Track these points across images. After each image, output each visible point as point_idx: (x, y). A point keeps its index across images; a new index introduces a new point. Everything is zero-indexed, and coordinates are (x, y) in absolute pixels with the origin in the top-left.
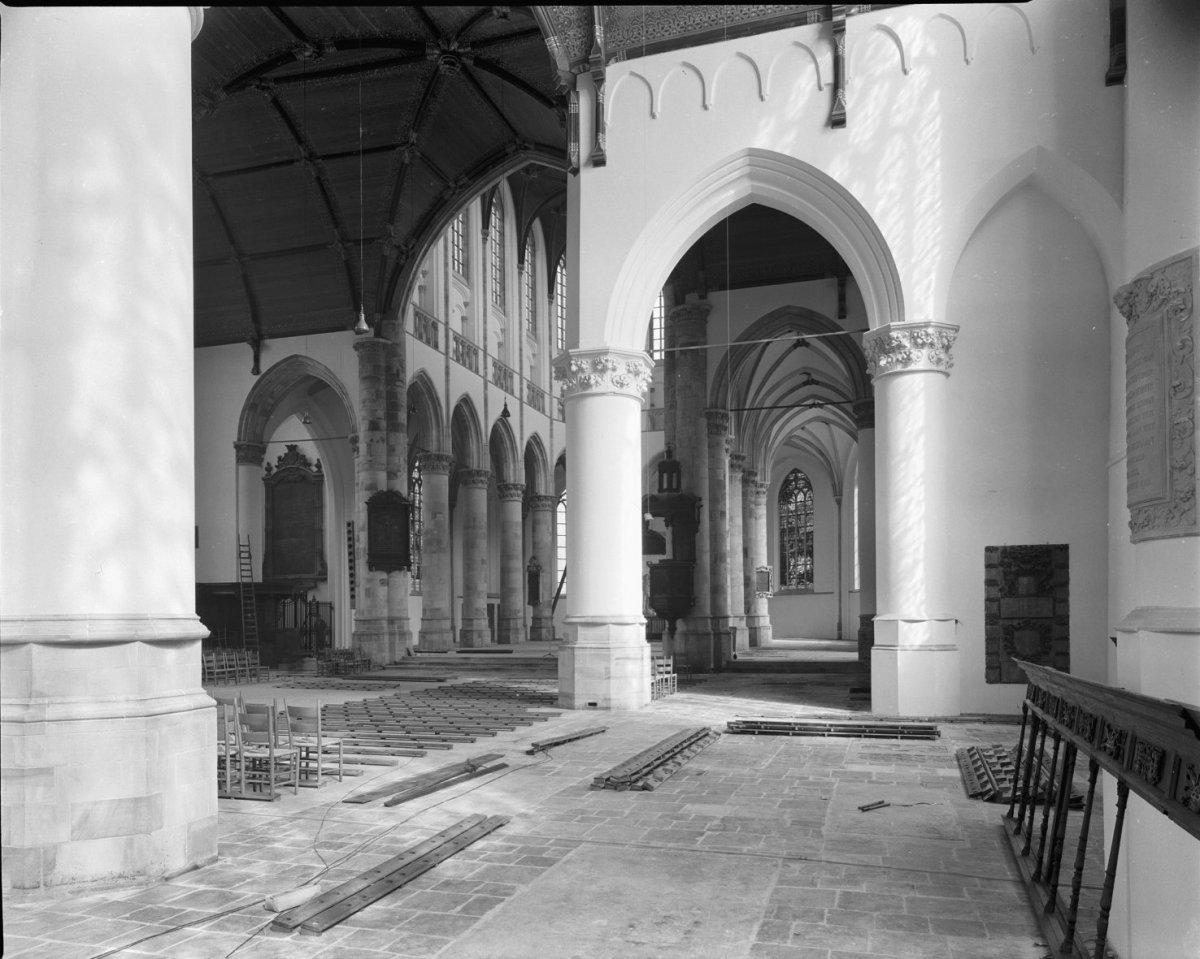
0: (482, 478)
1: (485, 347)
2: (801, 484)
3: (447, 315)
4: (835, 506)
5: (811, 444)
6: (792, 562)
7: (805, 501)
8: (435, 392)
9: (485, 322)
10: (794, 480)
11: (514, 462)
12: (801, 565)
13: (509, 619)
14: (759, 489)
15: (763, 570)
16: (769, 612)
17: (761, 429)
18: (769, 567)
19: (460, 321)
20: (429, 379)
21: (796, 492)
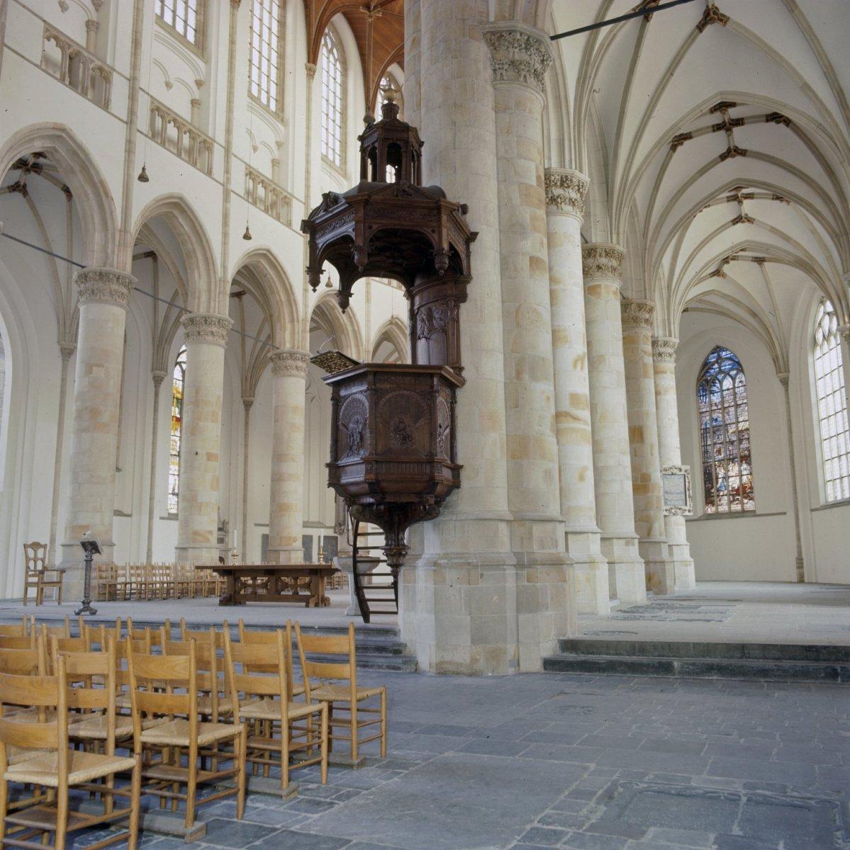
0: (214, 329)
1: (228, 142)
2: (727, 365)
3: (135, 66)
4: (779, 387)
5: (737, 303)
6: (721, 473)
7: (734, 388)
8: (97, 172)
9: (230, 110)
10: (717, 362)
11: (292, 321)
12: (734, 476)
13: (277, 551)
14: (662, 350)
15: (675, 471)
16: (688, 539)
17: (655, 240)
18: (684, 468)
19: (190, 106)
20: (80, 147)
21: (720, 377)
